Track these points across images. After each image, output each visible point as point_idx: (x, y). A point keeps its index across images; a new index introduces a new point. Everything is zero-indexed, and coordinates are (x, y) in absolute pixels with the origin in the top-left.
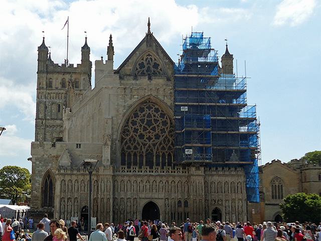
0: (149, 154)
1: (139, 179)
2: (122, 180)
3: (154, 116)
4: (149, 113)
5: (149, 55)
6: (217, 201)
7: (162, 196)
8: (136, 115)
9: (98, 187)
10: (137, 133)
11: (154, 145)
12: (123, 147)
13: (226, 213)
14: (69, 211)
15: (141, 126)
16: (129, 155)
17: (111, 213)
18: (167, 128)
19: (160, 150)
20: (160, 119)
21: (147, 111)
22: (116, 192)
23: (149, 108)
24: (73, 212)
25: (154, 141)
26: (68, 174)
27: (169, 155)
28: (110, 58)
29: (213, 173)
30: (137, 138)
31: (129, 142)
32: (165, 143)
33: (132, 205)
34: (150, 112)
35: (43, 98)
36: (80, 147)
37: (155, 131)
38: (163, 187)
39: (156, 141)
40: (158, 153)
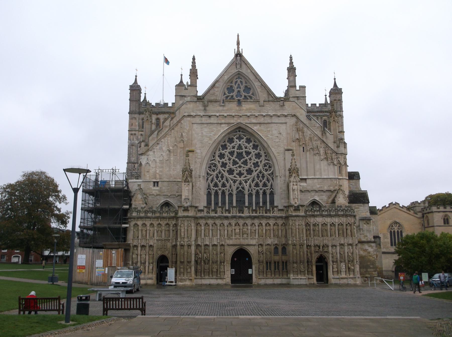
0: (240, 193)
1: (226, 222)
2: (207, 223)
4: (240, 145)
5: (239, 78)
6: (321, 247)
7: (254, 242)
8: (224, 147)
9: (177, 231)
10: (225, 168)
12: (209, 186)
13: (333, 262)
14: (143, 262)
15: (230, 159)
16: (216, 193)
17: (193, 262)
18: (261, 162)
20: (252, 151)
21: (237, 142)
22: (199, 238)
23: (240, 138)
24: (147, 263)
25: (246, 177)
26: (141, 218)
27: (264, 193)
28: (193, 85)
29: (316, 213)
30: (226, 174)
31: (215, 179)
33: (219, 253)
35: (135, 139)
36: (157, 186)
37: (247, 165)
38: (255, 230)
39: (249, 176)
40: (250, 191)
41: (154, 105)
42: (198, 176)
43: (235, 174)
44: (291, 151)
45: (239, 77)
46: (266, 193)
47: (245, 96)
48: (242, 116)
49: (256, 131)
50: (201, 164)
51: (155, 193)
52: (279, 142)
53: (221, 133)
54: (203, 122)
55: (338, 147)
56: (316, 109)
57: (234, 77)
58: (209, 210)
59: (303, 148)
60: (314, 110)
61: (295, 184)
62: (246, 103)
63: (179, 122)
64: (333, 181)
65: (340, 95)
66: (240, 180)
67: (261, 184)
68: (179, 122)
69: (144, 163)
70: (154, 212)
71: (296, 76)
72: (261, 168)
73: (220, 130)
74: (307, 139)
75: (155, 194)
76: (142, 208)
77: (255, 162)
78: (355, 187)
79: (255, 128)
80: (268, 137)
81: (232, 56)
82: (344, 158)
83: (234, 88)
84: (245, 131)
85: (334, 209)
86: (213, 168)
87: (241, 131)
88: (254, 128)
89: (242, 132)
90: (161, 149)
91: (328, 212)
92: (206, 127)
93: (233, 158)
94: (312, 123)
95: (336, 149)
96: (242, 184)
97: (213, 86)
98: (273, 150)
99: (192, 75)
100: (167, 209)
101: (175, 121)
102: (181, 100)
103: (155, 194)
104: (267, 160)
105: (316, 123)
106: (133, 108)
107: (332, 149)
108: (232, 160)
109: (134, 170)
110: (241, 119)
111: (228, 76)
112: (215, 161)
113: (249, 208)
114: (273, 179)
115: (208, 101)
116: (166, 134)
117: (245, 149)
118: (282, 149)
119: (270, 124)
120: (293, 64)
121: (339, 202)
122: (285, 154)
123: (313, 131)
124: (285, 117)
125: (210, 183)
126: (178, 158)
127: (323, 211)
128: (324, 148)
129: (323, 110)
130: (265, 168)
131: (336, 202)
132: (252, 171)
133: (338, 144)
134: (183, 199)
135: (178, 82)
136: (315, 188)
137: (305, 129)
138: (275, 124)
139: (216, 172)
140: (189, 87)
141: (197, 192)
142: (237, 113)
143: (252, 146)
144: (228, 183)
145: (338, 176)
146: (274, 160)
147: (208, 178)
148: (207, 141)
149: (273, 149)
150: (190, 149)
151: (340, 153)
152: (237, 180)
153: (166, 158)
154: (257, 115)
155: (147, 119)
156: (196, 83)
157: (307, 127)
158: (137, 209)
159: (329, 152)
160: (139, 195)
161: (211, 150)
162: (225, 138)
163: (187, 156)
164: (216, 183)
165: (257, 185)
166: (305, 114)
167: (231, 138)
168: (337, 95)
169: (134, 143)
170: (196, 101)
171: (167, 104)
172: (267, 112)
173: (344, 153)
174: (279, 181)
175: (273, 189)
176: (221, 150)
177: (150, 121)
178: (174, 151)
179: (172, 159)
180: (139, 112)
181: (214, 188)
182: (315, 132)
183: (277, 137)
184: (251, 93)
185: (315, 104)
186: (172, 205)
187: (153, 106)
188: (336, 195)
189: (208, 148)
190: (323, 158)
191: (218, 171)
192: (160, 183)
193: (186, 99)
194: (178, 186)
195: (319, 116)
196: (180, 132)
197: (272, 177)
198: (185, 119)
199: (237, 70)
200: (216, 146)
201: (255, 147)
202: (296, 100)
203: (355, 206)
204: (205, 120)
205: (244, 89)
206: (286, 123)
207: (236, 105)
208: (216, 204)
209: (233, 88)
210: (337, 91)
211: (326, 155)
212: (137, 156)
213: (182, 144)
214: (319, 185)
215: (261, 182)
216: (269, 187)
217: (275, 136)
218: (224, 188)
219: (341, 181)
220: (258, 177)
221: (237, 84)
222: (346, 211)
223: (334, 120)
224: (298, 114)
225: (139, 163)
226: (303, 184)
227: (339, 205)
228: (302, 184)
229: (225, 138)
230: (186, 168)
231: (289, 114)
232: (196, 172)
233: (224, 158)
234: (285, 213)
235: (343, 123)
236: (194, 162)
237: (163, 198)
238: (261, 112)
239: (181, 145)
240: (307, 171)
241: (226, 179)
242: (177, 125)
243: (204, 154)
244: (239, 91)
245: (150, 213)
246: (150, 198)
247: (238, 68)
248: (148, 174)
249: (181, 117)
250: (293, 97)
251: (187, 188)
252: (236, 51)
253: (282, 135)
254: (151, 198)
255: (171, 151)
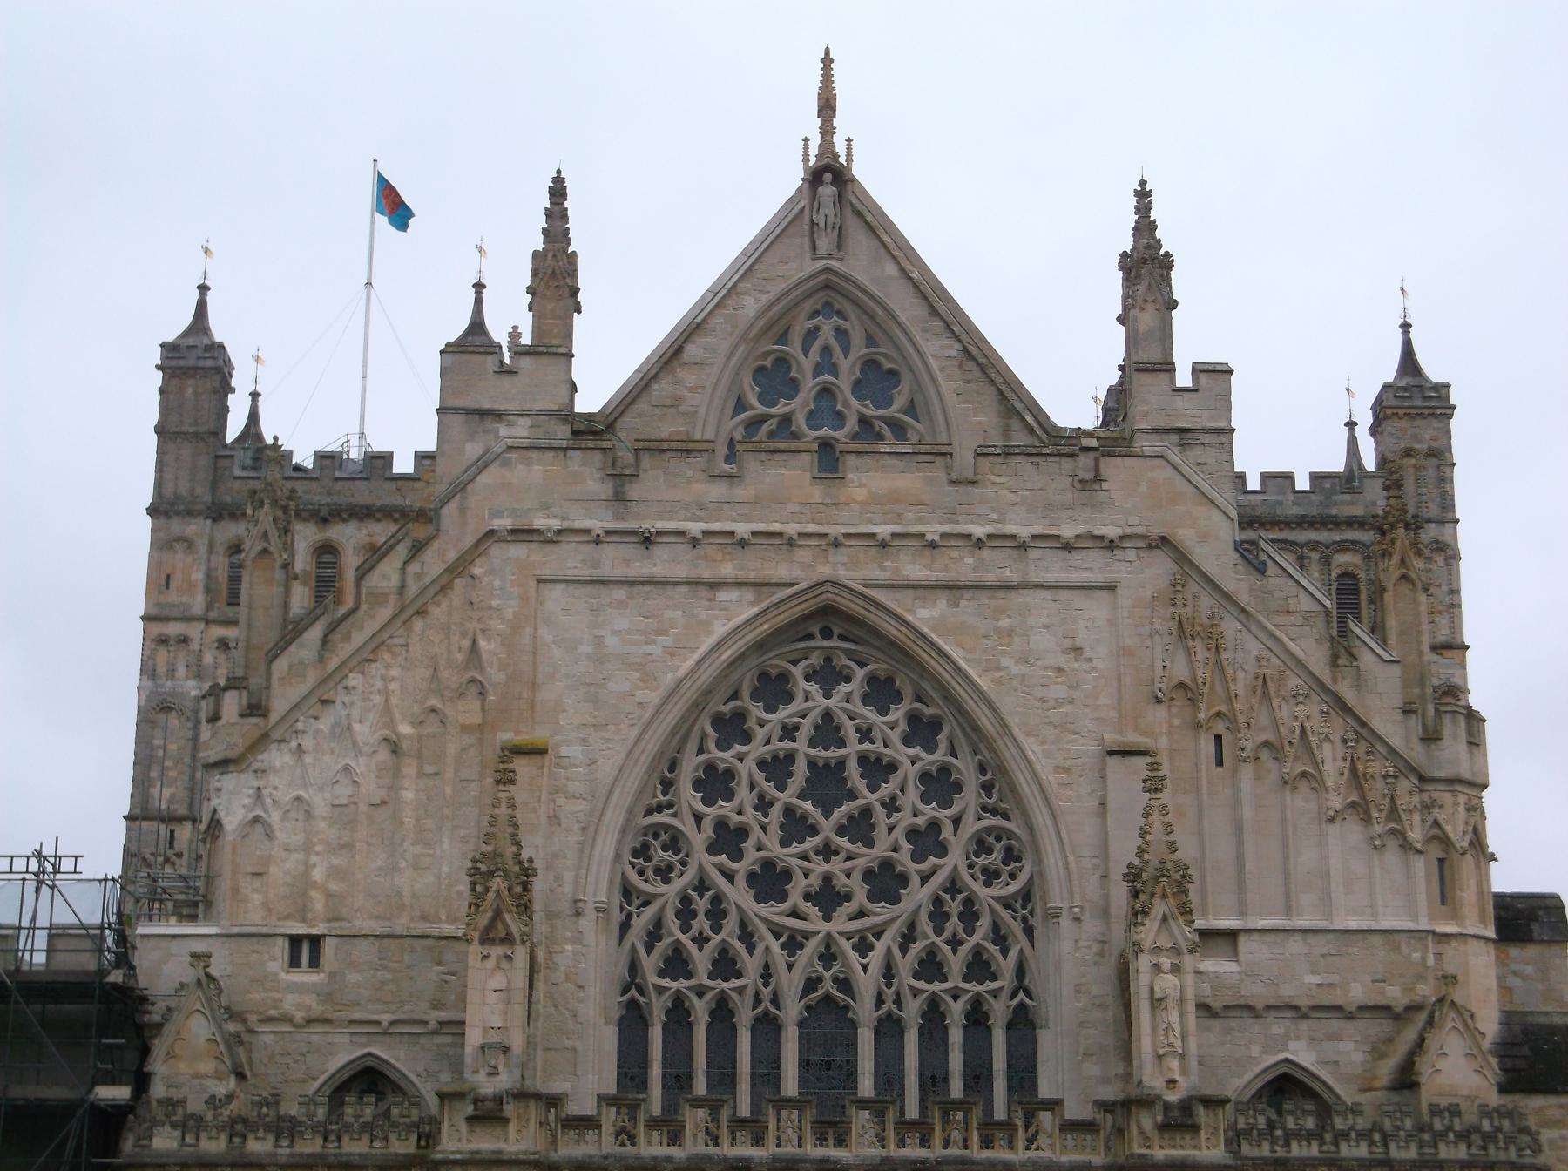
3: (865, 734)
4: (827, 715)
5: (828, 309)
8: (733, 728)
10: (737, 856)
11: (863, 948)
12: (634, 966)
15: (763, 805)
16: (679, 1013)
18: (957, 821)
19: (905, 978)
20: (901, 753)
21: (809, 699)
23: (828, 676)
25: (861, 914)
27: (977, 1018)
30: (739, 896)
31: (672, 924)
32: (939, 931)
34: (831, 702)
35: (181, 671)
36: (314, 963)
37: (869, 843)
40: (889, 1005)
41: (308, 463)
42: (565, 907)
43: (795, 898)
44: (1141, 762)
45: (828, 304)
46: (986, 1016)
47: (864, 421)
48: (841, 538)
49: (926, 630)
50: (590, 830)
51: (299, 1006)
52: (1072, 702)
53: (711, 641)
54: (608, 569)
55: (1431, 737)
56: (1295, 504)
57: (797, 304)
58: (633, 1119)
59: (1218, 739)
60: (1279, 511)
61: (1165, 961)
62: (869, 460)
63: (458, 568)
64: (1405, 949)
65: (1435, 424)
66: (829, 935)
67: (956, 963)
68: (458, 568)
69: (233, 817)
70: (286, 1128)
71: (1173, 304)
72: (955, 858)
73: (706, 626)
74: (1240, 687)
75: (299, 1016)
76: (212, 1102)
77: (920, 821)
78: (1540, 987)
79: (926, 615)
80: (998, 669)
81: (791, 179)
82: (1468, 810)
83: (800, 369)
84: (857, 632)
85: (1408, 1123)
86: (661, 855)
87: (836, 631)
88: (914, 614)
89: (842, 638)
90: (344, 731)
91: (1372, 1143)
92: (621, 605)
93: (788, 796)
94: (1271, 592)
95: (1416, 753)
96: (840, 960)
97: (671, 356)
98: (1029, 753)
99: (547, 287)
100: (369, 1113)
101: (433, 563)
102: (472, 436)
103: (299, 1016)
104: (995, 812)
105: (1294, 589)
106: (177, 478)
107: (1393, 751)
108: (776, 812)
109: (167, 860)
110: (840, 556)
111: (765, 299)
112: (674, 815)
113: (876, 1108)
114: (1029, 931)
115: (640, 445)
116: (377, 640)
117: (861, 742)
118: (1086, 747)
119: (1014, 594)
120: (1158, 234)
121: (1440, 1080)
122: (1103, 777)
123: (1277, 639)
124: (1108, 554)
125: (642, 952)
126: (448, 791)
127: (1345, 1135)
128: (1344, 741)
129: (1334, 512)
130: (983, 860)
131: (1423, 1080)
132: (903, 880)
133: (1430, 724)
134: (468, 1050)
135: (457, 327)
136: (1287, 992)
137: (1230, 627)
138: (1047, 594)
139: (678, 884)
140: (526, 363)
141: (556, 1007)
142: (813, 521)
143: (903, 726)
144: (751, 949)
145: (1432, 917)
146: (1040, 817)
147: (629, 916)
148: (626, 687)
149: (1032, 747)
150: (524, 737)
151: (1442, 774)
152: (807, 935)
153: (371, 788)
154: (936, 538)
155: (265, 551)
156: (568, 336)
157: (1243, 610)
158: (180, 1111)
159: (1377, 767)
160: (198, 1015)
161: (652, 745)
162: (735, 676)
163: (505, 778)
164: (678, 949)
165: (931, 967)
166: (1226, 532)
167: (774, 673)
168: (1419, 422)
169: (174, 694)
170: (564, 444)
171: (386, 459)
172: (997, 522)
173: (1466, 775)
174: (1067, 946)
175: (1028, 994)
176: (712, 745)
177: (279, 562)
178: (420, 750)
179: (409, 795)
180: (213, 503)
181: (666, 982)
182: (1292, 646)
183: (1059, 670)
184: (900, 401)
185: (1289, 477)
186: (403, 1084)
187: (298, 468)
188: (1420, 1043)
189: (635, 732)
190: (1338, 806)
191: (691, 873)
192: (329, 949)
193: (503, 431)
194: (439, 963)
195: (1313, 549)
196: (464, 635)
197: (1024, 919)
198: (496, 551)
199: (820, 264)
200: (683, 719)
201: (922, 730)
202: (1177, 449)
203: (1541, 1109)
204: (615, 561)
205: (858, 375)
206: (1111, 588)
207: (808, 476)
208: (678, 1080)
209: (789, 369)
210: (1418, 403)
211: (1360, 788)
212: (193, 778)
213: (476, 705)
214: (1313, 972)
215: (955, 951)
216: (1006, 981)
217: (1046, 668)
218: (726, 980)
219: (1450, 950)
220: (939, 915)
221: (816, 348)
222: (1488, 1138)
223: (1404, 577)
224: (1185, 536)
225: (206, 818)
226: (1218, 965)
227: (1444, 1102)
228: (1210, 965)
229: (735, 676)
230: (497, 855)
231: (1129, 531)
232: (558, 878)
233: (729, 796)
234: (1108, 1148)
235: (1455, 592)
236: (543, 820)
237: (346, 1039)
238: (961, 518)
239: (469, 711)
240: (1241, 887)
241: (743, 925)
242: (443, 587)
243: (607, 768)
244: (826, 392)
245: (261, 1133)
246: (266, 1039)
247: (822, 251)
248: (256, 890)
249: (469, 541)
250: (1155, 431)
251: (498, 981)
252: (814, 150)
253: (1090, 660)
254: (269, 1039)
255: (405, 745)
